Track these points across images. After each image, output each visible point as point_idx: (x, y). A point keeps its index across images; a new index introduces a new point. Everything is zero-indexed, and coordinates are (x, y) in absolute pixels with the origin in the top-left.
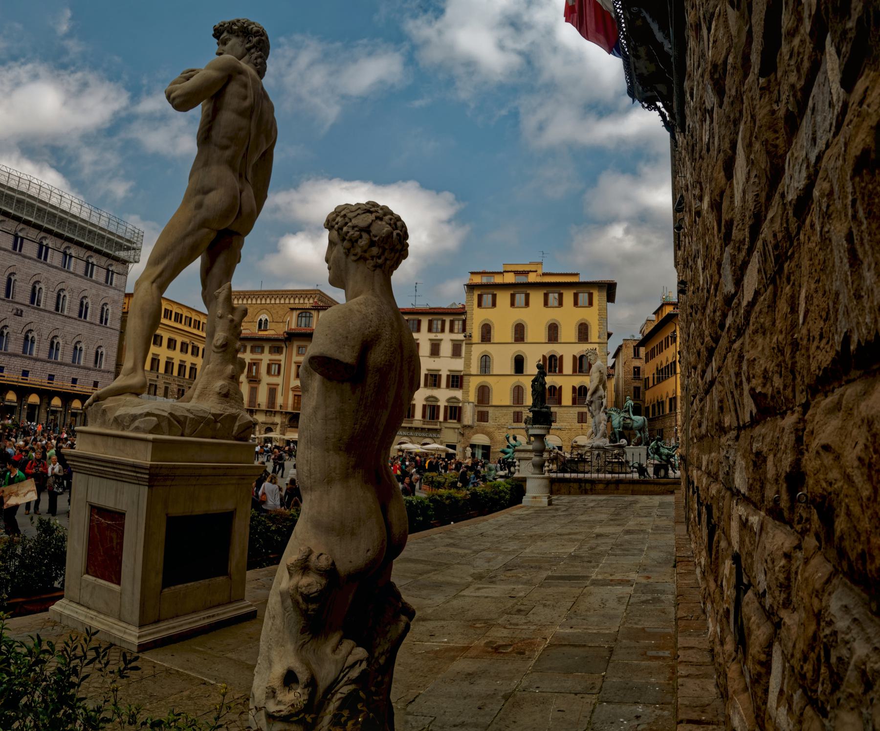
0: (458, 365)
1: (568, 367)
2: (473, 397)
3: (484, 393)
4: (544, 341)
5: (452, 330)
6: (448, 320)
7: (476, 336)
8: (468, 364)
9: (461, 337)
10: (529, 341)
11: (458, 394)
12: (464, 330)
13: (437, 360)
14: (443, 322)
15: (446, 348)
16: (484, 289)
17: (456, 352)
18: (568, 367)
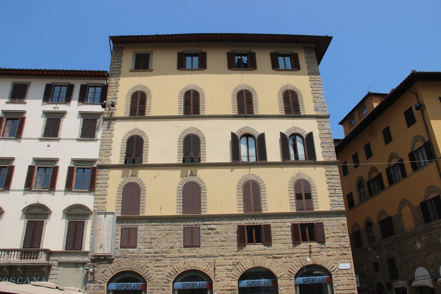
0: (90, 151)
1: (274, 153)
2: (113, 202)
3: (132, 195)
4: (231, 113)
5: (82, 99)
6: (78, 84)
7: (122, 107)
8: (106, 149)
9: (98, 108)
10: (207, 113)
11: (86, 200)
12: (104, 97)
13: (52, 143)
14: (70, 88)
15: (71, 125)
16: (139, 50)
17: (88, 130)
18: (274, 153)
